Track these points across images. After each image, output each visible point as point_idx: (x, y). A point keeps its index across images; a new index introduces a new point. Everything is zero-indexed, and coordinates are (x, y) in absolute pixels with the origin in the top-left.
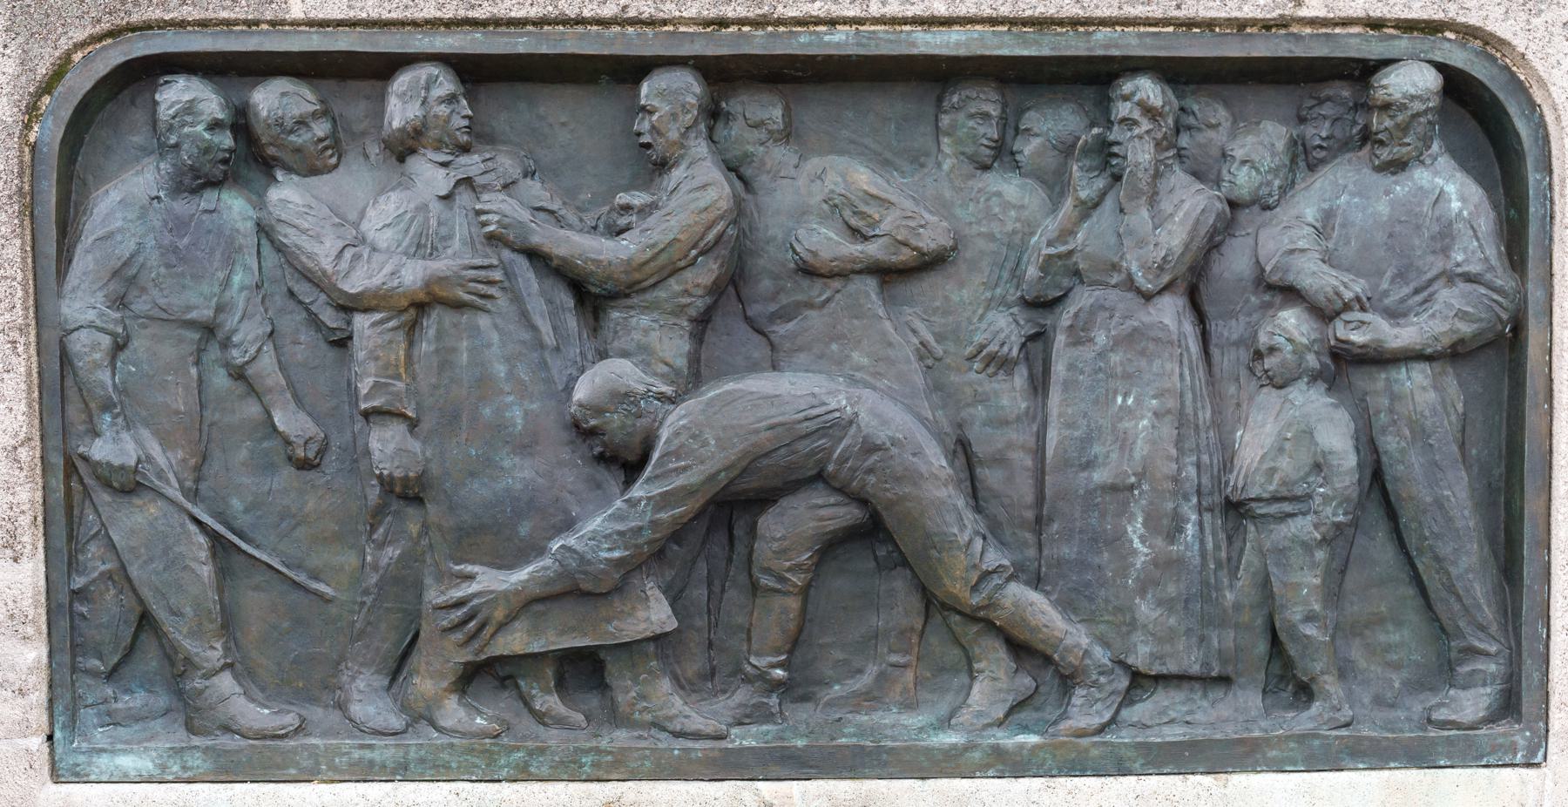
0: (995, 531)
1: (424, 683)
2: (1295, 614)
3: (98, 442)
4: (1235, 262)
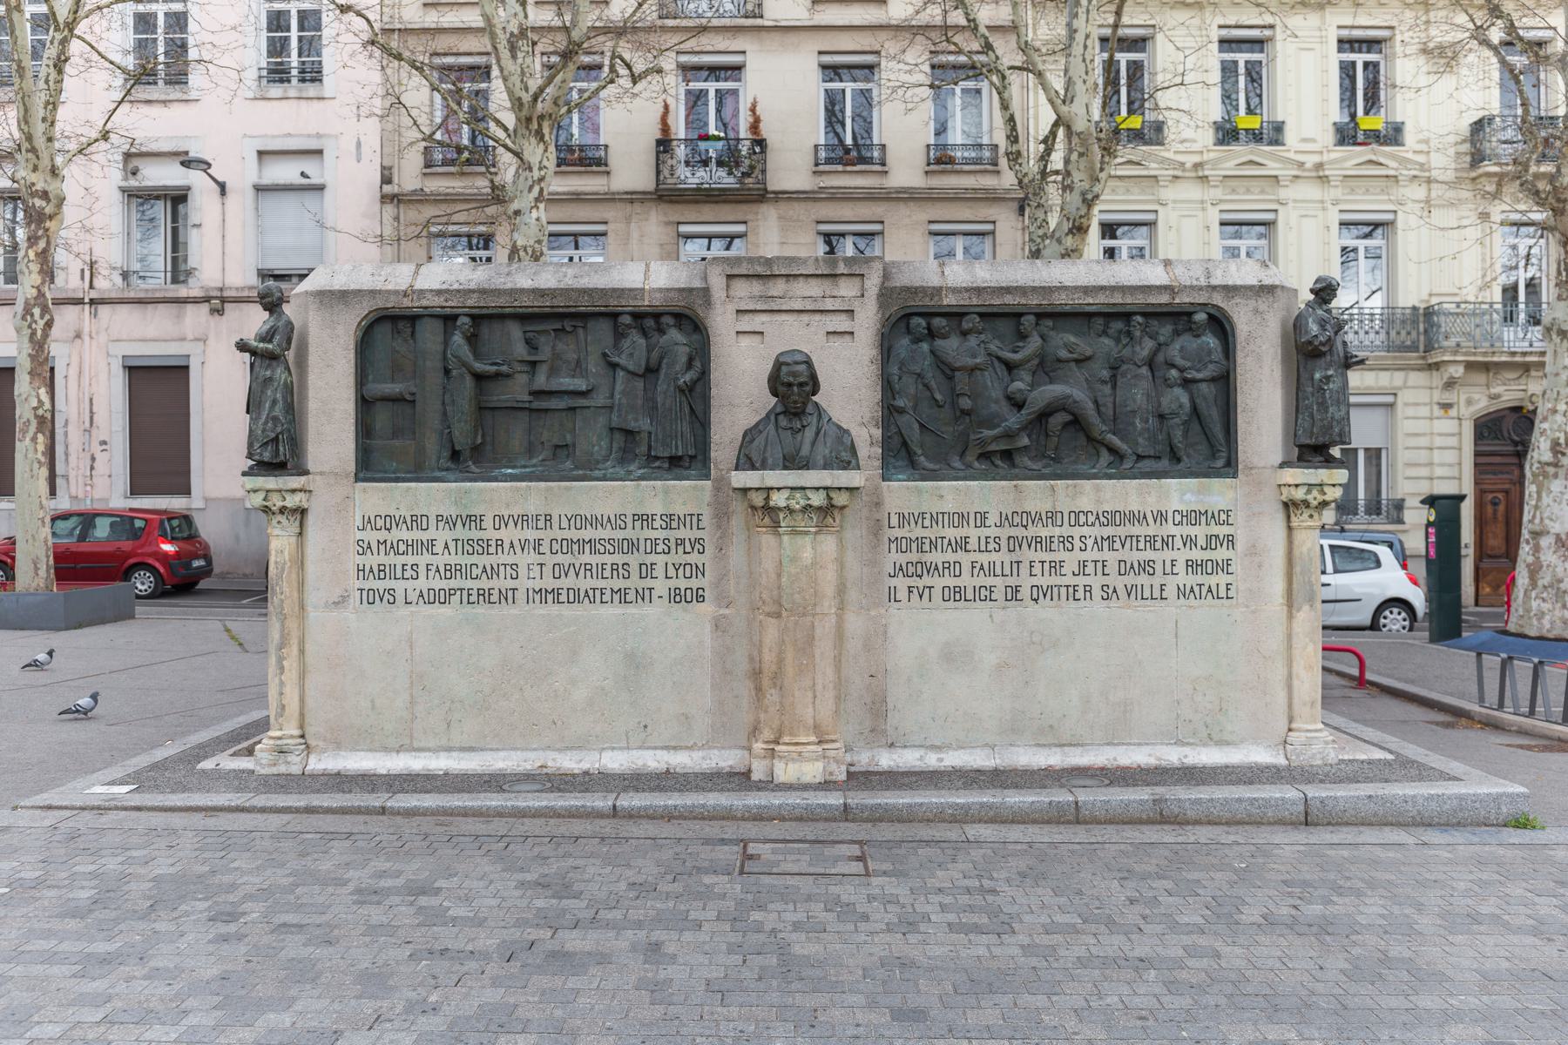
0: (1104, 422)
1: (970, 457)
2: (1176, 441)
4: (1160, 358)
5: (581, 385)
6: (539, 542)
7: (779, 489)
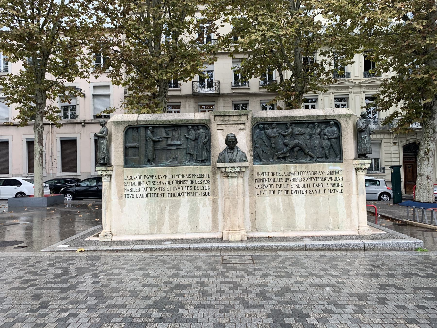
0: (308, 149)
1: (274, 159)
4: (322, 133)
5: (179, 143)
6: (169, 182)
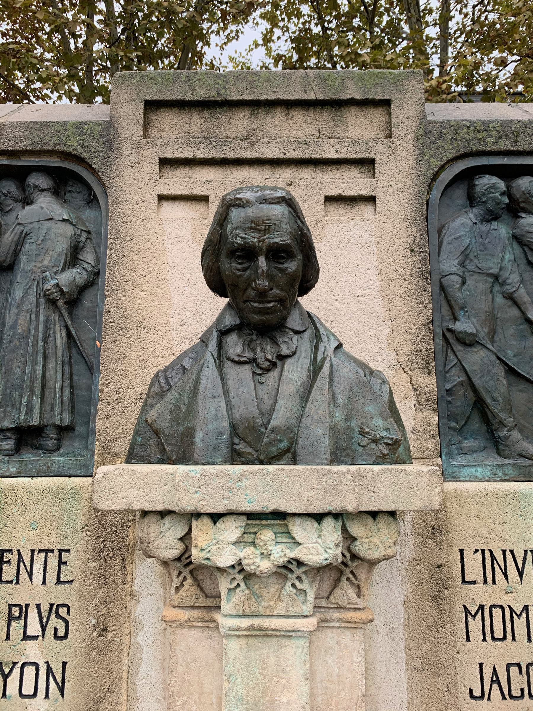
3: (457, 323)
7: (215, 517)
